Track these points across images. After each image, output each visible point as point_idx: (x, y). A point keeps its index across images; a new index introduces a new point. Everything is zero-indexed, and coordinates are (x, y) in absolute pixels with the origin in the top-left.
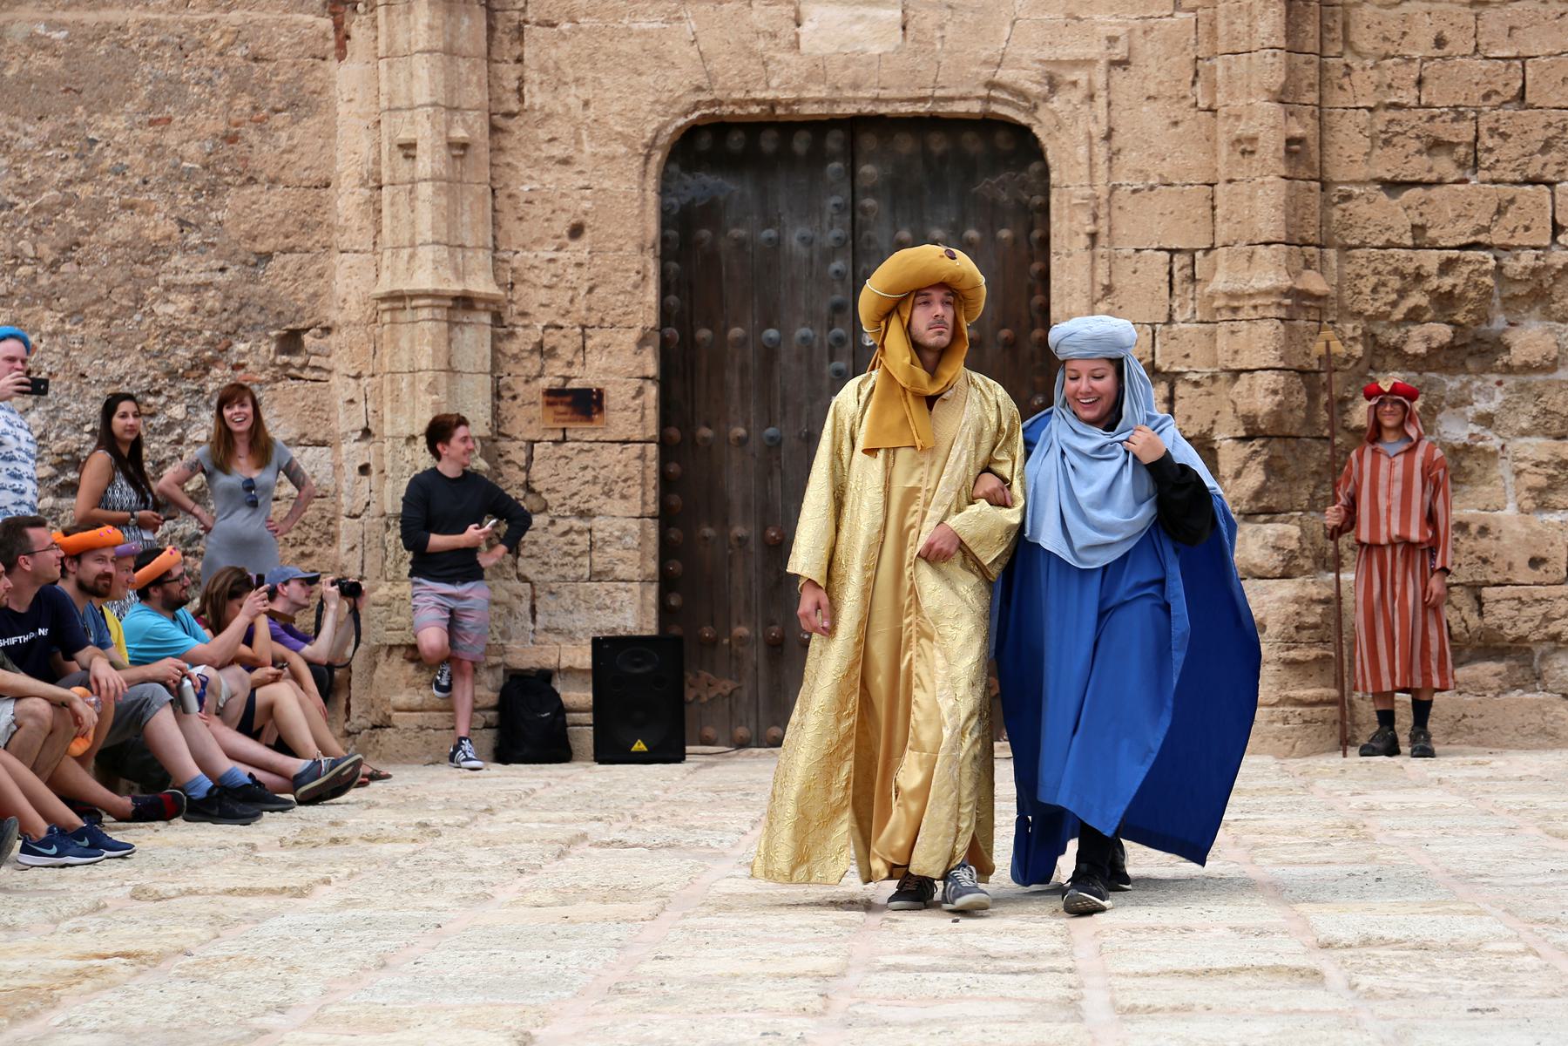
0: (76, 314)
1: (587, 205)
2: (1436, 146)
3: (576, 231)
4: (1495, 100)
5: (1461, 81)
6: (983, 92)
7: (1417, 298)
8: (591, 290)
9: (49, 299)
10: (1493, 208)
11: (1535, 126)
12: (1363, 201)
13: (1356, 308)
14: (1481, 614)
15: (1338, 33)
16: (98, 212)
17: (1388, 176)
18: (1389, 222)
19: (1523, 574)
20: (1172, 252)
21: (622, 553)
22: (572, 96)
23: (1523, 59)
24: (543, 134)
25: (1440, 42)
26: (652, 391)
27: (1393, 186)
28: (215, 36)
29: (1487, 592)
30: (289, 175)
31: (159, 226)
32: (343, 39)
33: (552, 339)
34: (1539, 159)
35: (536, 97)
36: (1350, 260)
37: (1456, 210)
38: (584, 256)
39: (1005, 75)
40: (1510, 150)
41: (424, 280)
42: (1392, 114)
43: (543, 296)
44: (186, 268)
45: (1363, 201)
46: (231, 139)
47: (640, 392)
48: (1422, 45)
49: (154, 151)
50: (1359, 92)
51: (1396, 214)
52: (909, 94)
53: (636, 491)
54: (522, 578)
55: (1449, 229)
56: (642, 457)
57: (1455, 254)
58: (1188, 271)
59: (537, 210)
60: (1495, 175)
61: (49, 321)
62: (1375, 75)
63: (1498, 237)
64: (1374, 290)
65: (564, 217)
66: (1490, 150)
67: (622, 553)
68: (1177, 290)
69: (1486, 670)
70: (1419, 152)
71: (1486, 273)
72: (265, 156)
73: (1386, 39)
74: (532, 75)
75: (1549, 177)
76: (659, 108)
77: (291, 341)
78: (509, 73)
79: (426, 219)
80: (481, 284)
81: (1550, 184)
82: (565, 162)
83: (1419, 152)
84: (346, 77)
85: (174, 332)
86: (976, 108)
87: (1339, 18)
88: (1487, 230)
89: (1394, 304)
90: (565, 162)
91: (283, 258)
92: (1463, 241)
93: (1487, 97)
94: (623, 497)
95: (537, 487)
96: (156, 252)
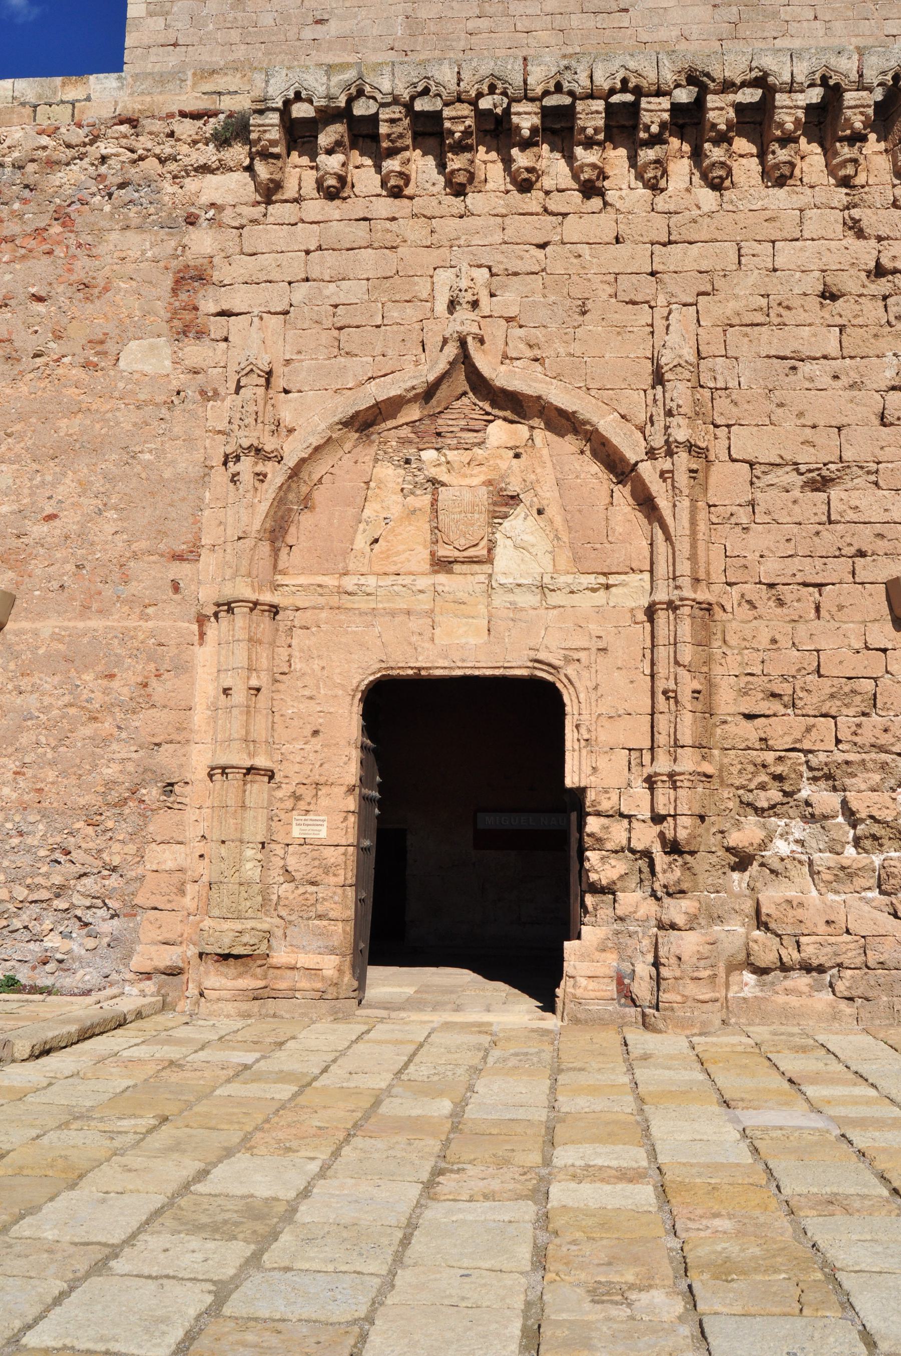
0: (63, 773)
1: (321, 720)
3: (316, 733)
4: (804, 672)
6: (530, 664)
7: (763, 778)
8: (321, 765)
9: (53, 763)
10: (804, 729)
12: (733, 724)
13: (729, 782)
14: (799, 951)
15: (719, 635)
17: (747, 712)
18: (746, 736)
19: (822, 928)
20: (630, 750)
21: (333, 906)
22: (316, 665)
23: (818, 651)
24: (300, 684)
25: (774, 641)
26: (352, 819)
27: (749, 717)
28: (140, 634)
29: (803, 940)
30: (172, 704)
32: (202, 635)
33: (301, 790)
34: (828, 704)
35: (297, 665)
36: (726, 756)
37: (784, 729)
38: (318, 747)
39: (542, 656)
42: (750, 678)
43: (297, 768)
44: (119, 750)
45: (733, 724)
47: (345, 819)
48: (765, 642)
50: (730, 667)
51: (750, 731)
52: (491, 665)
53: (342, 872)
54: (281, 917)
55: (780, 741)
56: (345, 854)
57: (783, 754)
58: (639, 761)
59: (295, 723)
60: (804, 712)
61: (51, 775)
62: (739, 658)
63: (806, 745)
64: (740, 772)
65: (309, 726)
66: (801, 699)
67: (333, 906)
68: (633, 770)
70: (763, 699)
71: (800, 764)
73: (744, 639)
74: (296, 654)
75: (834, 714)
76: (360, 671)
77: (169, 788)
81: (834, 717)
82: (311, 698)
83: (763, 699)
85: (110, 784)
86: (524, 672)
87: (719, 628)
88: (800, 741)
89: (750, 780)
90: (311, 698)
91: (167, 746)
92: (787, 747)
93: (799, 670)
94: (335, 875)
95: (289, 869)
96: (106, 741)
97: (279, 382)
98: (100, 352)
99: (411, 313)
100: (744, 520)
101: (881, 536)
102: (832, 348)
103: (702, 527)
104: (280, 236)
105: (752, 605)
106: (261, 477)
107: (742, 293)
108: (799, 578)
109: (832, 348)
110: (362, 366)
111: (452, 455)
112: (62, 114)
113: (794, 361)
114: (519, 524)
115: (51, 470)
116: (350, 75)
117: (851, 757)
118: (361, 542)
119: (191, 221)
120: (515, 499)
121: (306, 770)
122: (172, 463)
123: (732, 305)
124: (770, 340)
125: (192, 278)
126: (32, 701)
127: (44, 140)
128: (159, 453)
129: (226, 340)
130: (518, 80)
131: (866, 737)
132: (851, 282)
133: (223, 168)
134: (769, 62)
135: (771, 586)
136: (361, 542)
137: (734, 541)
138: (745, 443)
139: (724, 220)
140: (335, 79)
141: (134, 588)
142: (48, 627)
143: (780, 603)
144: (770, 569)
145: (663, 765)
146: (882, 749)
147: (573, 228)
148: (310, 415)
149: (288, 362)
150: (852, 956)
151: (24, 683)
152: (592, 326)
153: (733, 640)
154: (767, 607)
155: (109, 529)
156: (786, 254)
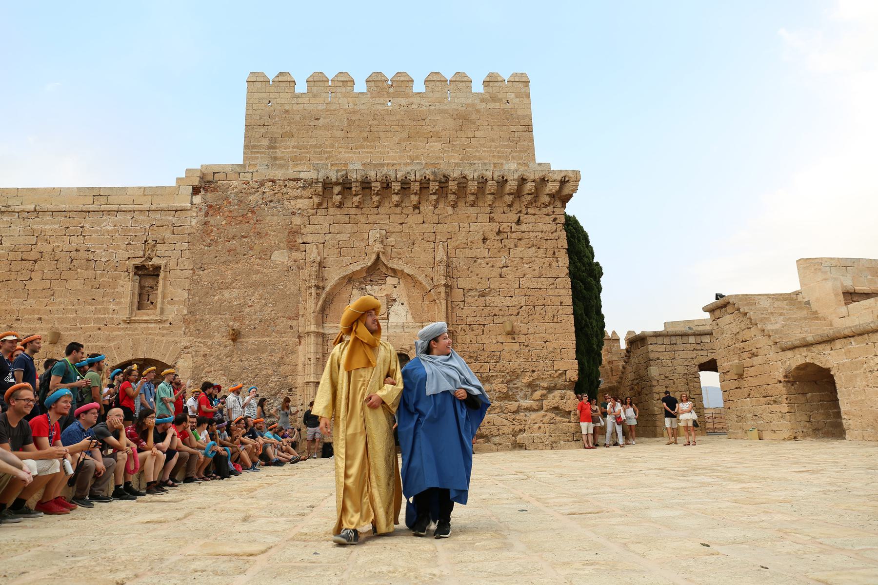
2: (471, 357)
5: (474, 347)
9: (253, 383)
11: (486, 354)
16: (261, 369)
31: (270, 372)
32: (300, 342)
40: (482, 358)
41: (312, 380)
49: (270, 360)
69: (481, 440)
72: (287, 360)
77: (290, 390)
78: (326, 347)
79: (312, 370)
84: (300, 348)
85: (272, 389)
96: (270, 376)
98: (265, 254)
99: (363, 244)
102: (486, 255)
103: (450, 308)
104: (321, 221)
107: (461, 238)
109: (486, 255)
110: (347, 259)
111: (375, 287)
112: (249, 176)
113: (475, 259)
114: (396, 307)
115: (250, 291)
119: (293, 214)
120: (395, 300)
123: (458, 242)
124: (468, 253)
125: (295, 232)
126: (246, 364)
127: (245, 186)
128: (285, 286)
131: (498, 368)
132: (492, 236)
133: (302, 197)
134: (466, 172)
138: (462, 283)
139: (455, 217)
141: (278, 328)
142: (251, 340)
144: (470, 320)
146: (503, 372)
147: (411, 219)
148: (333, 277)
150: (495, 432)
151: (243, 358)
152: (416, 248)
153: (459, 341)
154: (468, 331)
155: (270, 309)
156: (473, 227)
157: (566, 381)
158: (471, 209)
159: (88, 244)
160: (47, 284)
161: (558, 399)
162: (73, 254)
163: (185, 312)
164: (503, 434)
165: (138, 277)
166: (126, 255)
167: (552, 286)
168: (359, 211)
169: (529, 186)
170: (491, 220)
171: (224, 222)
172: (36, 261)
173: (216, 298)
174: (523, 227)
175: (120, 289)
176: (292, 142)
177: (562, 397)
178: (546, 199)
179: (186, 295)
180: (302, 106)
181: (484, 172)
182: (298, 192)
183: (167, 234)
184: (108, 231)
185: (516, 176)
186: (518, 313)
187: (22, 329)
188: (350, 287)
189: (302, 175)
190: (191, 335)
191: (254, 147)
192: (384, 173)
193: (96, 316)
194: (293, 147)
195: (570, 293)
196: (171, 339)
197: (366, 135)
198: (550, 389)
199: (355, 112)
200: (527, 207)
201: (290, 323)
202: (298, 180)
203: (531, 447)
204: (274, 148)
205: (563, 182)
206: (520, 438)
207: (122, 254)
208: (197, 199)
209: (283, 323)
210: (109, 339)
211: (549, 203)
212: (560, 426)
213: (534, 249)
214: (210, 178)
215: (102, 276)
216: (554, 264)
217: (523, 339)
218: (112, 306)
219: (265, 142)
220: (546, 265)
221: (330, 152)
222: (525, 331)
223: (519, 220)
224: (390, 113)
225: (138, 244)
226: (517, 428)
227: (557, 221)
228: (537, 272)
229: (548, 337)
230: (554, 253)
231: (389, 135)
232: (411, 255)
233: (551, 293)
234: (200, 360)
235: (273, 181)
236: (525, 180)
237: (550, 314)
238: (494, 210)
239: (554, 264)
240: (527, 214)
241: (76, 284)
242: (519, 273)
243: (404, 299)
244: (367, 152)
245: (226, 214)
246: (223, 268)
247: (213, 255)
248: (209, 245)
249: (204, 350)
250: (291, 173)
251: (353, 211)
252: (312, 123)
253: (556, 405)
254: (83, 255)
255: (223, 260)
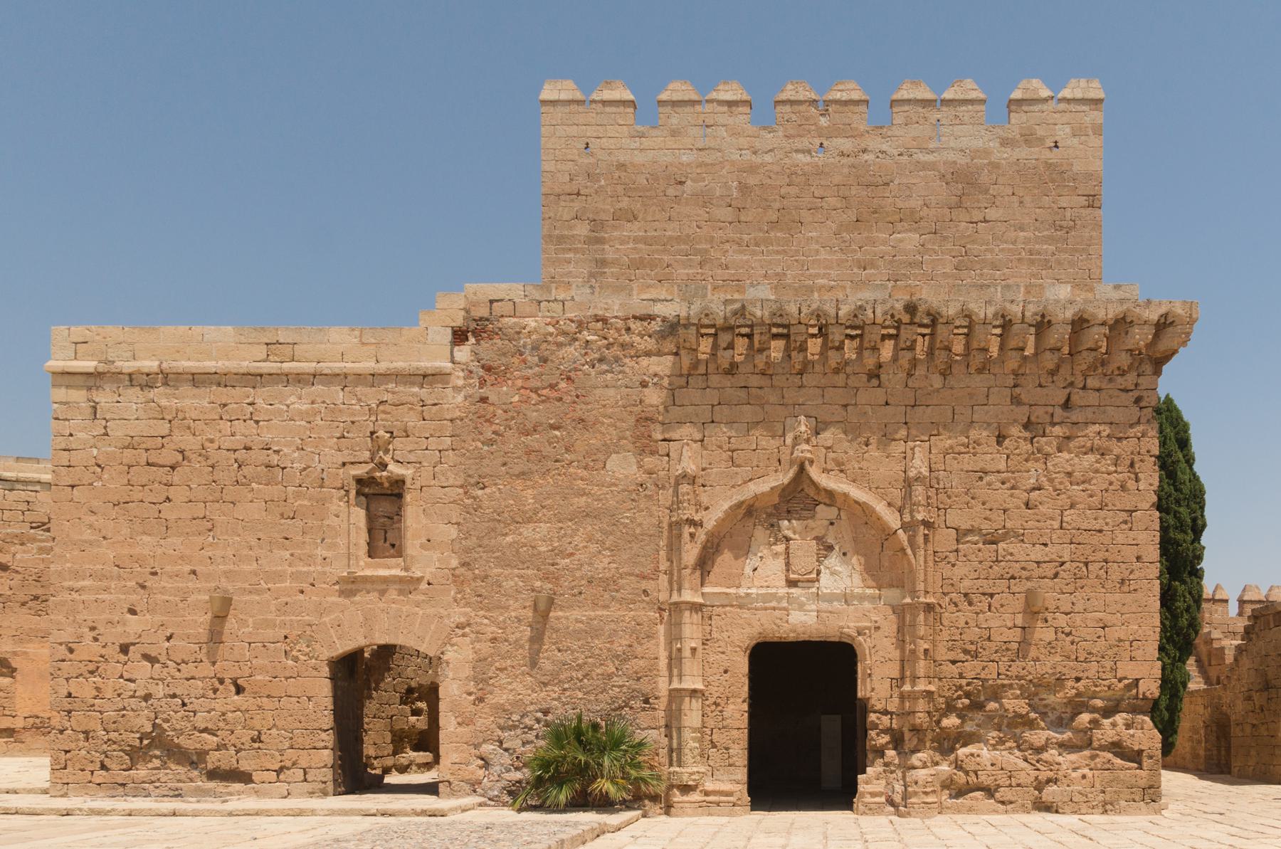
3: (726, 672)
7: (960, 692)
11: (993, 646)
19: (990, 768)
22: (725, 635)
27: (954, 662)
35: (715, 635)
37: (971, 668)
44: (617, 681)
46: (630, 646)
48: (962, 624)
51: (954, 670)
63: (983, 676)
77: (646, 701)
80: (700, 686)
96: (610, 676)
97: (700, 481)
100: (953, 560)
101: (1023, 569)
102: (1002, 466)
105: (956, 606)
106: (692, 535)
108: (981, 590)
109: (1002, 466)
116: (737, 306)
117: (1006, 682)
118: (748, 570)
121: (721, 689)
122: (640, 525)
124: (968, 462)
128: (633, 520)
129: (668, 455)
130: (832, 312)
135: (966, 595)
136: (748, 570)
137: (947, 571)
138: (955, 518)
140: (729, 308)
143: (970, 604)
144: (966, 585)
145: (907, 687)
149: (703, 470)
153: (945, 622)
155: (606, 560)
157: (1136, 697)
158: (978, 378)
159: (267, 437)
160: (199, 510)
161: (1121, 727)
162: (241, 454)
163: (454, 563)
164: (1018, 785)
165: (363, 498)
166: (338, 460)
167: (1124, 526)
168: (764, 381)
169: (1096, 335)
170: (1016, 401)
171: (516, 398)
172: (173, 468)
173: (509, 539)
174: (1076, 416)
175: (332, 521)
176: (634, 229)
177: (1128, 726)
178: (1123, 360)
179: (453, 532)
180: (651, 154)
181: (1008, 305)
182: (650, 344)
183: (412, 420)
184: (300, 412)
185: (1069, 314)
186: (1056, 575)
187: (163, 591)
188: (750, 523)
189: (659, 309)
190: (468, 604)
191: (561, 239)
192: (814, 306)
193: (294, 570)
194: (636, 240)
195: (1157, 540)
196: (431, 611)
197: (774, 218)
198: (1108, 712)
199: (752, 169)
200: (1085, 377)
201: (644, 585)
202: (650, 318)
203: (1067, 809)
204: (600, 241)
205: (1163, 325)
206: (1050, 793)
207: (331, 456)
208: (463, 353)
209: (629, 584)
210: (321, 611)
211: (1130, 367)
212: (1122, 774)
213: (1091, 458)
214: (483, 312)
215: (298, 496)
216: (1131, 484)
217: (1062, 620)
218: (320, 552)
219: (582, 230)
220: (1116, 486)
221: (706, 251)
222: (1067, 608)
223: (1068, 400)
224: (820, 172)
225: (359, 438)
226: (1044, 776)
227: (1143, 404)
228: (1095, 501)
229: (1108, 618)
230: (1132, 465)
231: (819, 217)
232: (864, 464)
233: (1120, 538)
234: (485, 648)
235: (604, 320)
236: (1088, 321)
237: (1116, 576)
238: (1021, 380)
239: (1131, 484)
240: (1084, 388)
241: (253, 510)
242: (1063, 500)
243: (849, 547)
244: (778, 252)
245: (519, 383)
246: (519, 484)
247: (501, 460)
248: (490, 442)
249: (492, 630)
250: (637, 301)
251: (755, 381)
252: (671, 192)
253: (1116, 739)
254: (258, 456)
255: (517, 470)
